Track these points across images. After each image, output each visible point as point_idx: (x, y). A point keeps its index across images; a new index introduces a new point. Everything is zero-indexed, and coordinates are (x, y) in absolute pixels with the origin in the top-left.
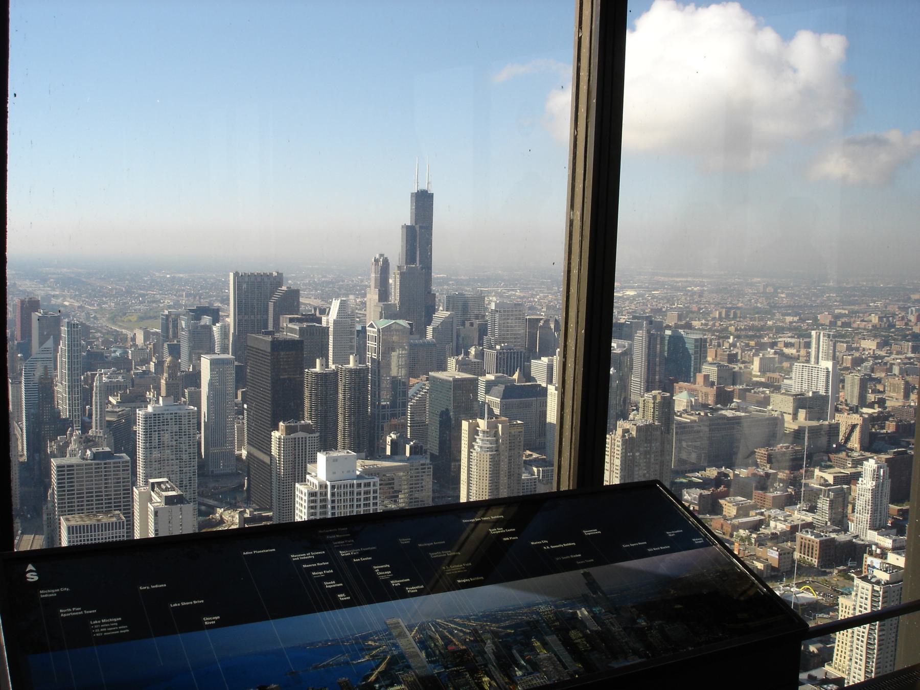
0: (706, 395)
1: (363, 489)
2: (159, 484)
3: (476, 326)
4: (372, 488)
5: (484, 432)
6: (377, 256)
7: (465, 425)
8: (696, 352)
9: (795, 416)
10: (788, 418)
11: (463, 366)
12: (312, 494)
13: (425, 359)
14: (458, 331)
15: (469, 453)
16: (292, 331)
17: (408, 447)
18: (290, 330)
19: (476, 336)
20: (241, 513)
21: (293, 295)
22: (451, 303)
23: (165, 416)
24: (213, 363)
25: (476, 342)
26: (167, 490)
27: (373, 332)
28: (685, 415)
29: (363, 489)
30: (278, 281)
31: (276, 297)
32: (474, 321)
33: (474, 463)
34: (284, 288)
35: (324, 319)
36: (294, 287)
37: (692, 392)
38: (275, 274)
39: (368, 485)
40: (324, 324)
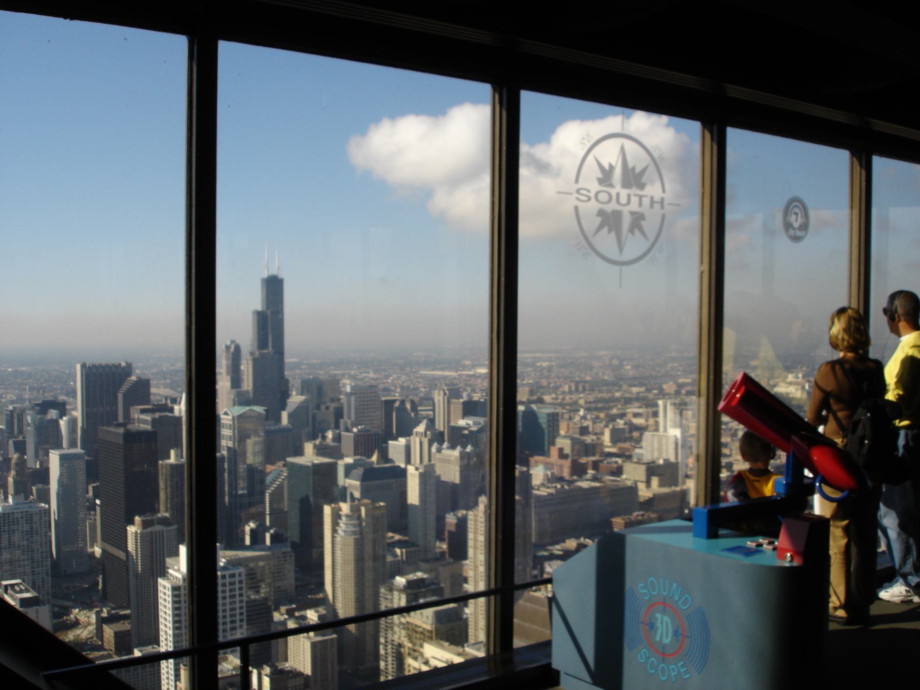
0: (561, 467)
1: (227, 580)
2: (12, 586)
3: (331, 409)
4: (237, 579)
5: (347, 516)
6: (229, 343)
7: (327, 510)
8: (549, 426)
9: (648, 483)
10: (641, 486)
11: (321, 450)
12: (175, 589)
13: (281, 445)
14: (314, 416)
15: (333, 538)
16: (145, 422)
17: (268, 536)
18: (142, 421)
19: (332, 419)
20: (98, 613)
21: (143, 386)
22: (306, 387)
23: (16, 515)
24: (64, 459)
25: (333, 425)
26: (21, 591)
27: (228, 420)
28: (542, 489)
29: (227, 580)
30: (127, 371)
31: (125, 387)
32: (329, 404)
33: (338, 547)
34: (134, 378)
35: (176, 408)
36: (143, 377)
37: (548, 466)
38: (123, 364)
39: (233, 576)
40: (176, 413)
